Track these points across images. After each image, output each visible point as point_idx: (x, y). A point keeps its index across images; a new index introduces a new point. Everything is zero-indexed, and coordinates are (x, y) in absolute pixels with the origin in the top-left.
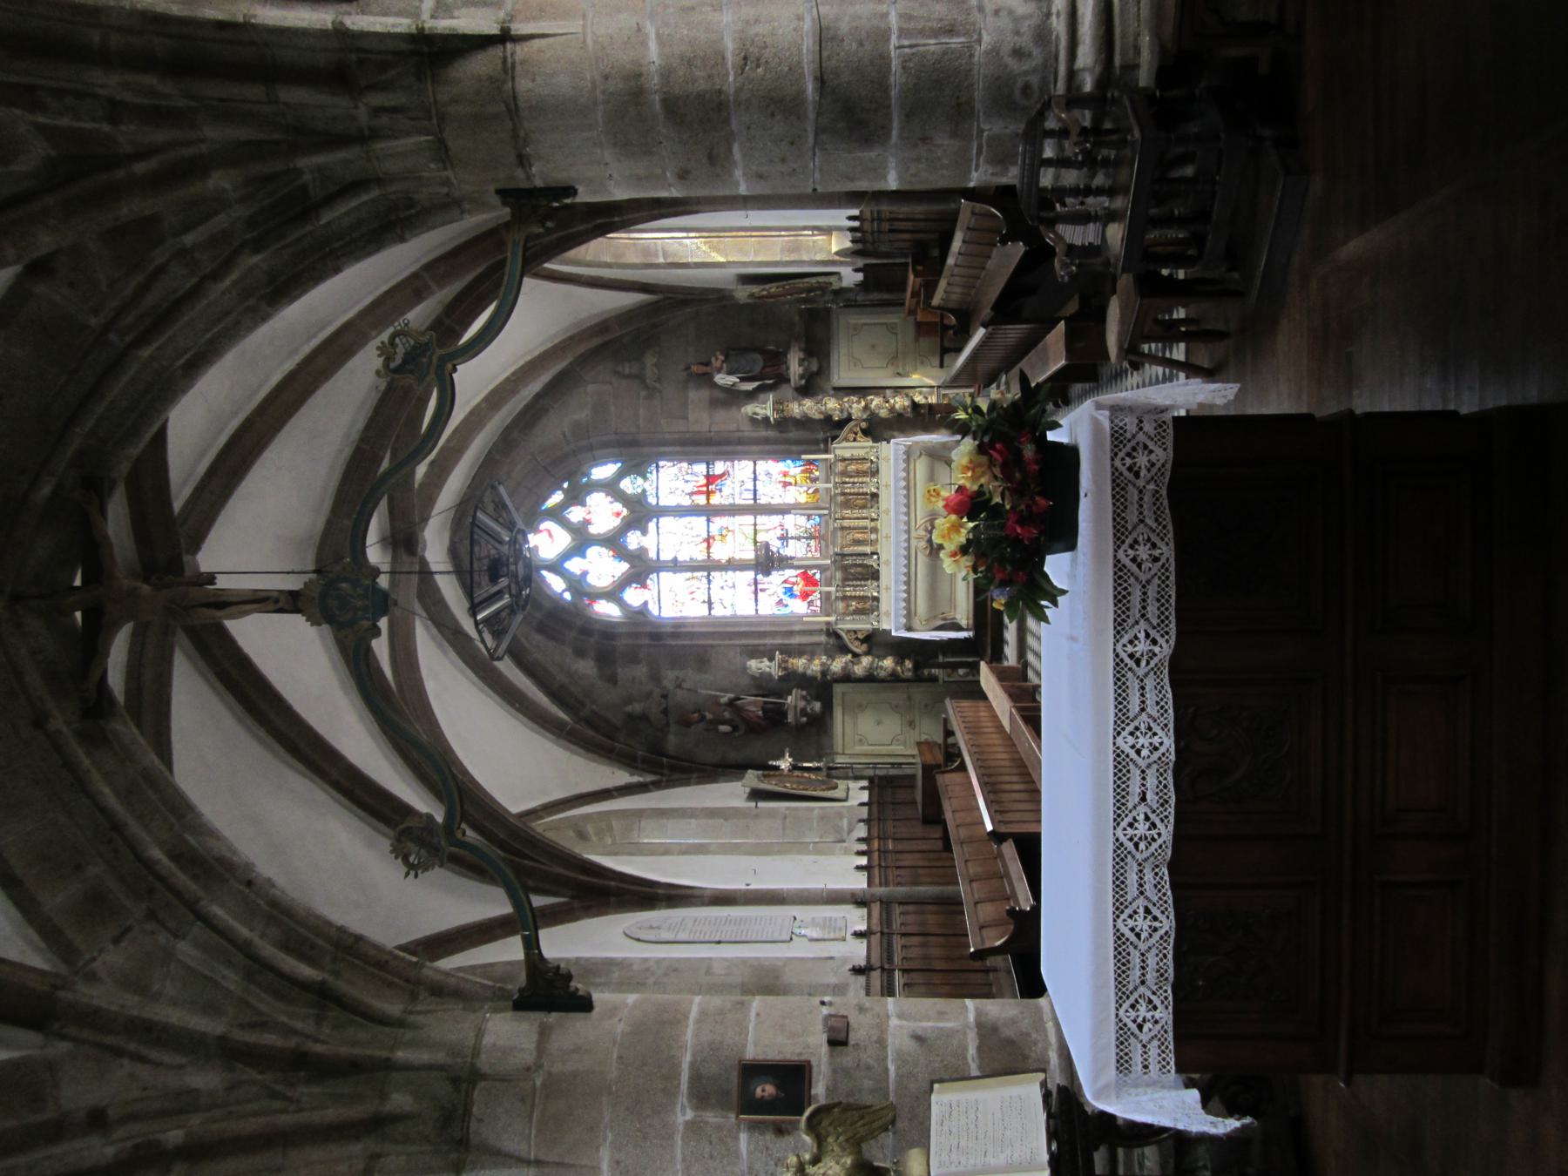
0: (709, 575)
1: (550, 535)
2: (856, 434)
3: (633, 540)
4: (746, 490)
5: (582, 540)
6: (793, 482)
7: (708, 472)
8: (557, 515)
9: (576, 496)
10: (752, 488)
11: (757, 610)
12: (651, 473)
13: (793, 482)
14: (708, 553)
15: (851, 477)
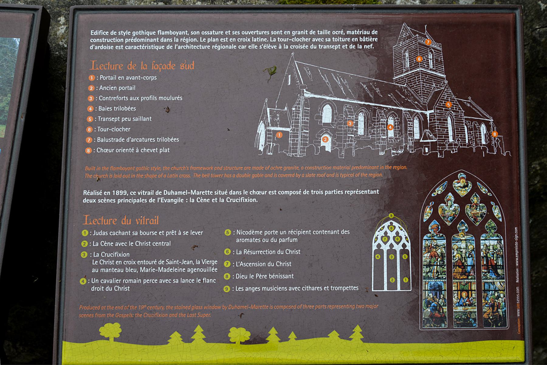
1: (464, 187)
3: (463, 227)
4: (489, 285)
5: (462, 201)
6: (495, 311)
8: (475, 189)
9: (485, 200)
13: (495, 311)
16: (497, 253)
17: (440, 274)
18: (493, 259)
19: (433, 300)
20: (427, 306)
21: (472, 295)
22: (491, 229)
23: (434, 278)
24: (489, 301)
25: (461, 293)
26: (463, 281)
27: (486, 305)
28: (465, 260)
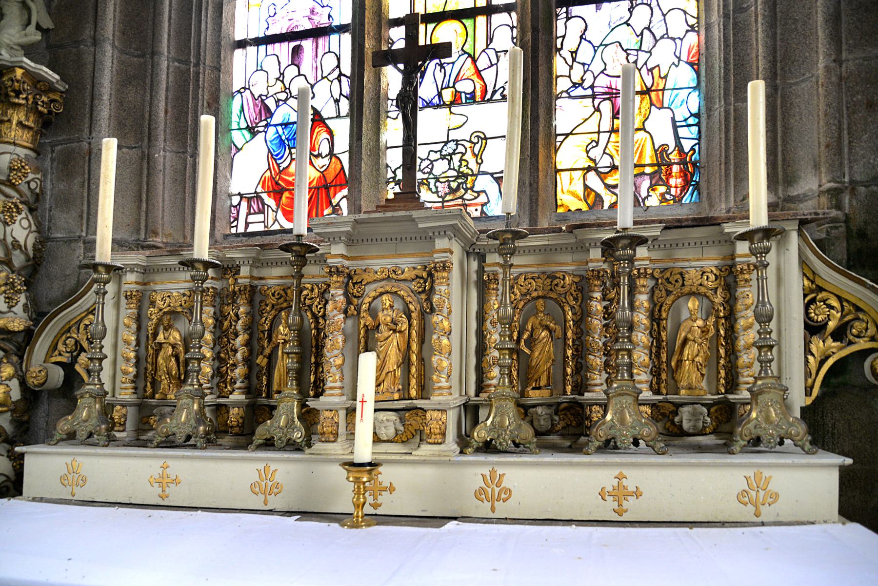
2: (839, 334)
11: (242, 44)
15: (655, 317)
27: (579, 91)
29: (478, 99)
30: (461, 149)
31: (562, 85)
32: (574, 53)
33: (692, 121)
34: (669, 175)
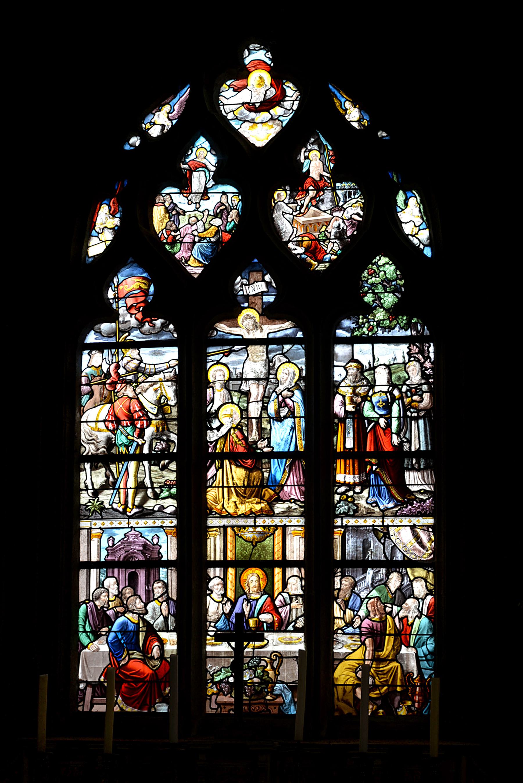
0: (172, 457)
7: (410, 454)
10: (370, 557)
12: (408, 326)
14: (222, 456)
16: (407, 400)
17: (149, 492)
18: (389, 425)
19: (122, 604)
20: (92, 632)
21: (285, 585)
22: (380, 289)
23: (124, 512)
24: (362, 613)
25: (238, 578)
26: (250, 522)
27: (350, 630)
28: (261, 430)
29: (276, 628)
30: (263, 663)
31: (339, 623)
32: (346, 603)
33: (429, 657)
34: (414, 693)
